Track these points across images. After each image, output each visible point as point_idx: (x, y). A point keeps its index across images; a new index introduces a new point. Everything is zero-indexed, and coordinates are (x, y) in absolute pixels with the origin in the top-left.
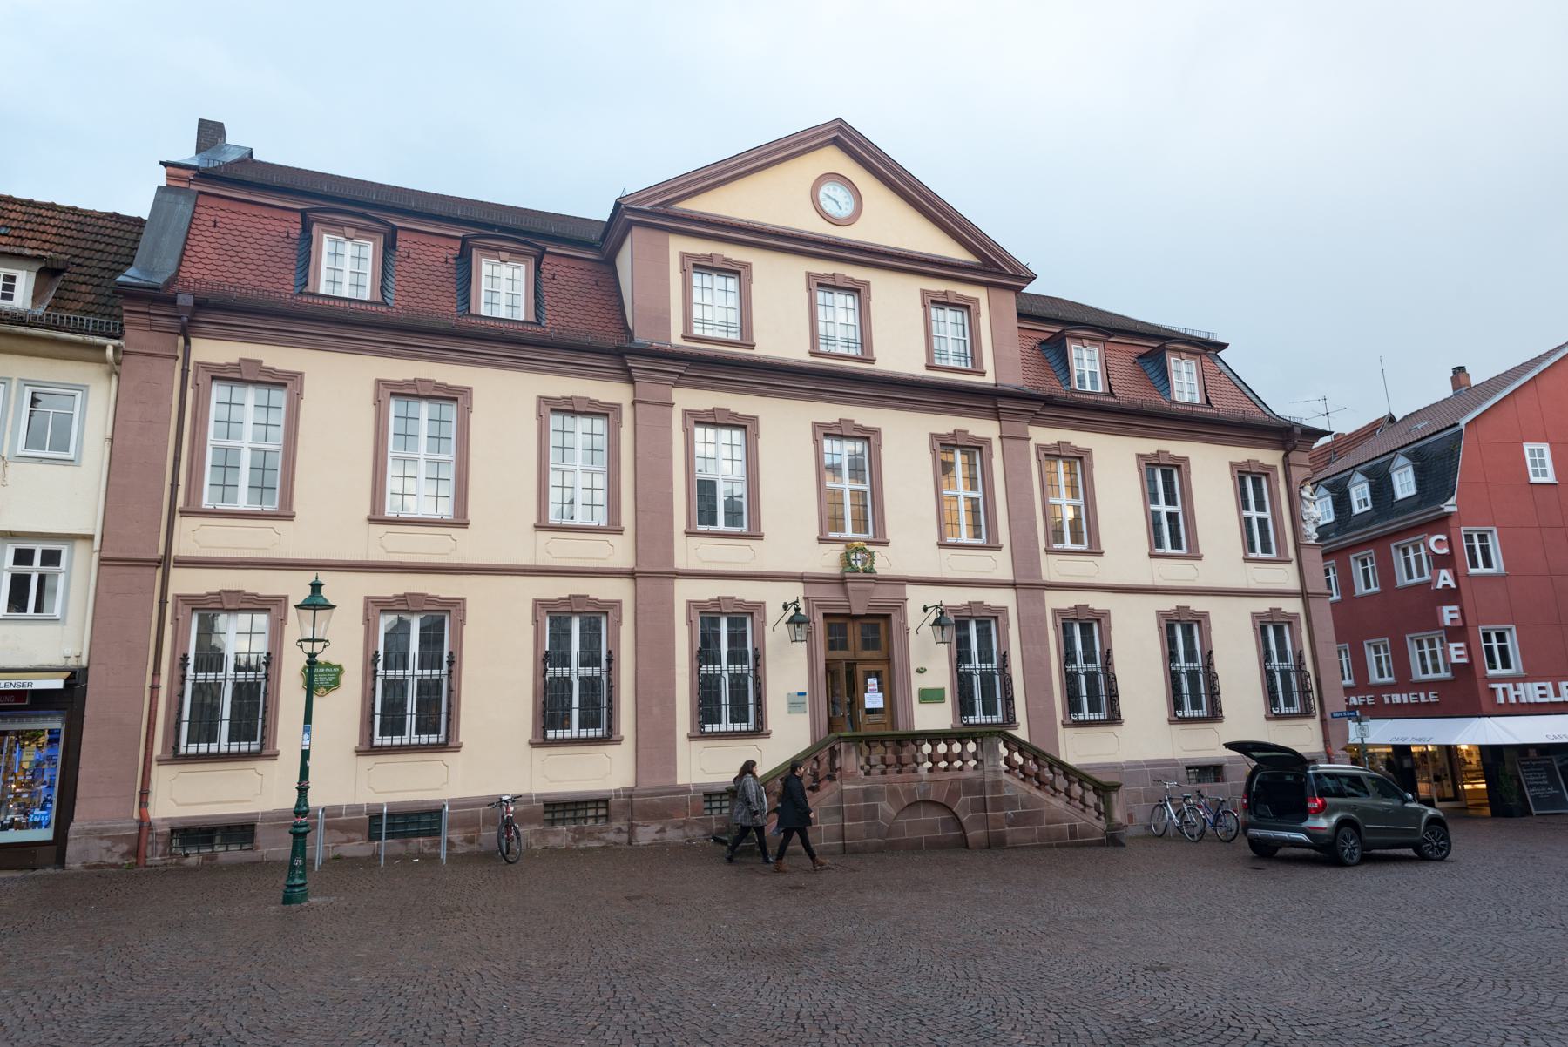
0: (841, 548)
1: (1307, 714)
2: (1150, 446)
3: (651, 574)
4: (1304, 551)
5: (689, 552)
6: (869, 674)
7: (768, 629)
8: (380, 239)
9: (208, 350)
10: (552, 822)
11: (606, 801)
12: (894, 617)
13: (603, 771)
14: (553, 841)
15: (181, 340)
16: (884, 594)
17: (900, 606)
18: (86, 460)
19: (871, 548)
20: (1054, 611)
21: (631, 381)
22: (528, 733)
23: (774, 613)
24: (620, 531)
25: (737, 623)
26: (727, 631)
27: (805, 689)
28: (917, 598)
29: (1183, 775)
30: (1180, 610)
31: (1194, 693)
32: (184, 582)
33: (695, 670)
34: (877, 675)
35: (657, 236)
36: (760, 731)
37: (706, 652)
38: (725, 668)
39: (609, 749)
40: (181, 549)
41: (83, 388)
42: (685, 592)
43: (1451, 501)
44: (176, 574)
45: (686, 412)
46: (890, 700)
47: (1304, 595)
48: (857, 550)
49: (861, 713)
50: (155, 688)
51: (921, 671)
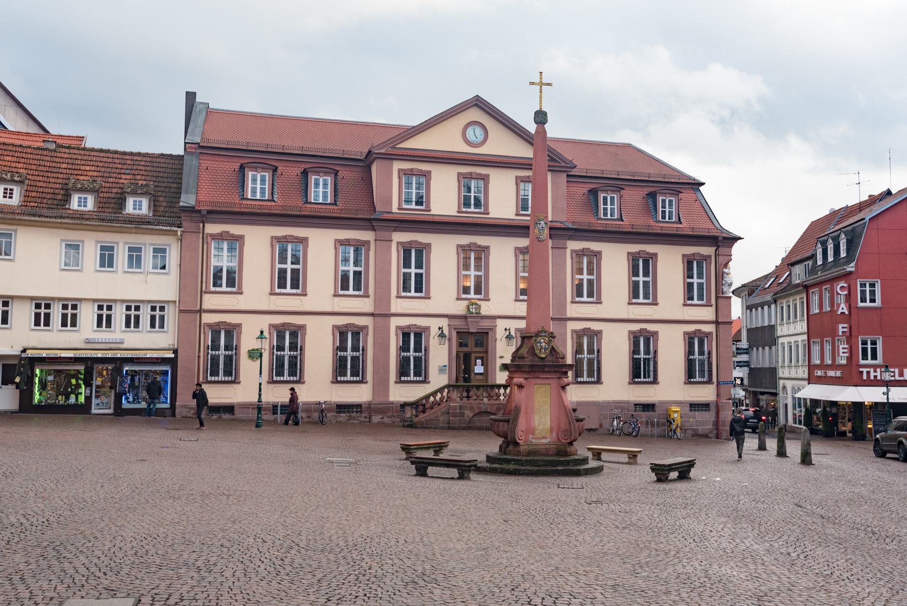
0: (466, 303)
1: (710, 381)
2: (635, 248)
3: (382, 315)
4: (720, 300)
5: (397, 305)
6: (477, 358)
7: (431, 338)
8: (271, 172)
9: (212, 228)
10: (339, 412)
11: (360, 406)
12: (490, 333)
13: (360, 394)
14: (340, 419)
15: (201, 225)
16: (485, 324)
17: (493, 329)
18: (172, 273)
19: (479, 302)
20: (572, 331)
21: (375, 230)
22: (330, 377)
23: (434, 331)
24: (368, 297)
25: (418, 336)
26: (414, 339)
27: (447, 364)
28: (501, 325)
29: (633, 408)
30: (641, 330)
31: (642, 369)
32: (207, 318)
33: (398, 355)
34: (482, 358)
35: (387, 162)
36: (425, 381)
37: (405, 347)
38: (412, 354)
39: (363, 385)
40: (206, 306)
41: (170, 245)
42: (395, 322)
43: (853, 264)
44: (204, 315)
45: (398, 243)
46: (486, 369)
47: (717, 323)
48: (472, 304)
49: (472, 375)
50: (199, 357)
51: (501, 357)
